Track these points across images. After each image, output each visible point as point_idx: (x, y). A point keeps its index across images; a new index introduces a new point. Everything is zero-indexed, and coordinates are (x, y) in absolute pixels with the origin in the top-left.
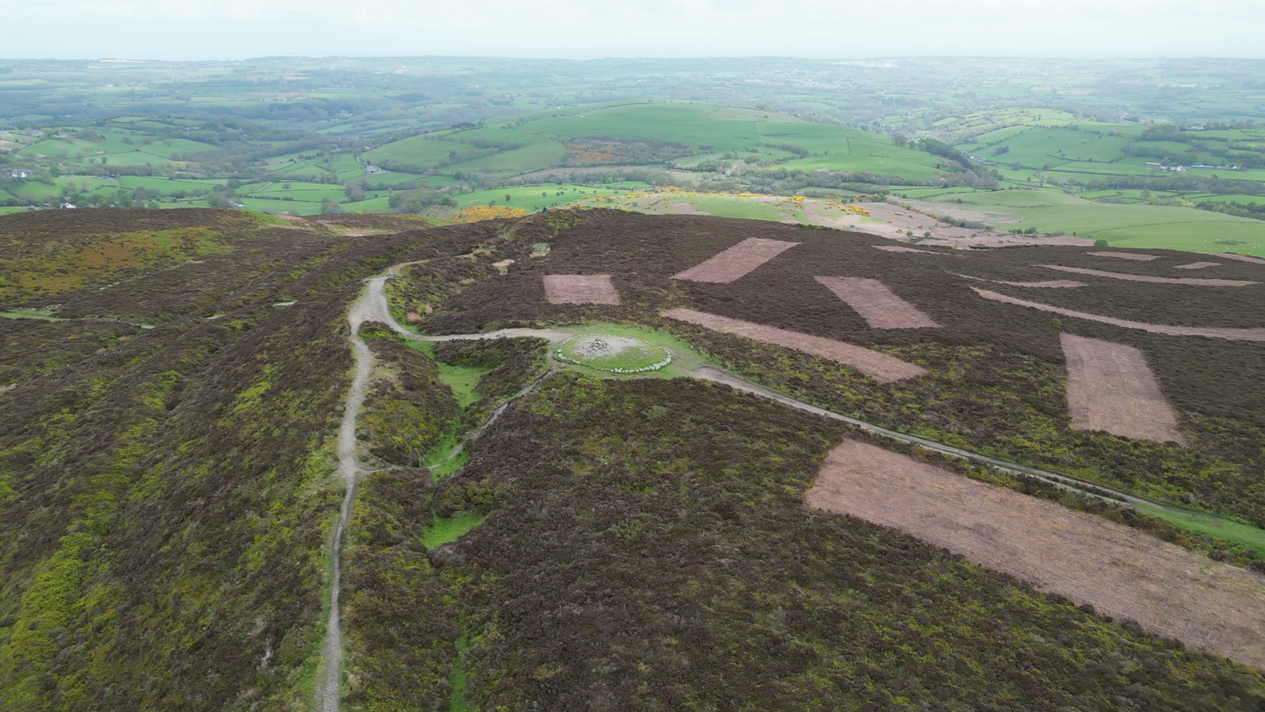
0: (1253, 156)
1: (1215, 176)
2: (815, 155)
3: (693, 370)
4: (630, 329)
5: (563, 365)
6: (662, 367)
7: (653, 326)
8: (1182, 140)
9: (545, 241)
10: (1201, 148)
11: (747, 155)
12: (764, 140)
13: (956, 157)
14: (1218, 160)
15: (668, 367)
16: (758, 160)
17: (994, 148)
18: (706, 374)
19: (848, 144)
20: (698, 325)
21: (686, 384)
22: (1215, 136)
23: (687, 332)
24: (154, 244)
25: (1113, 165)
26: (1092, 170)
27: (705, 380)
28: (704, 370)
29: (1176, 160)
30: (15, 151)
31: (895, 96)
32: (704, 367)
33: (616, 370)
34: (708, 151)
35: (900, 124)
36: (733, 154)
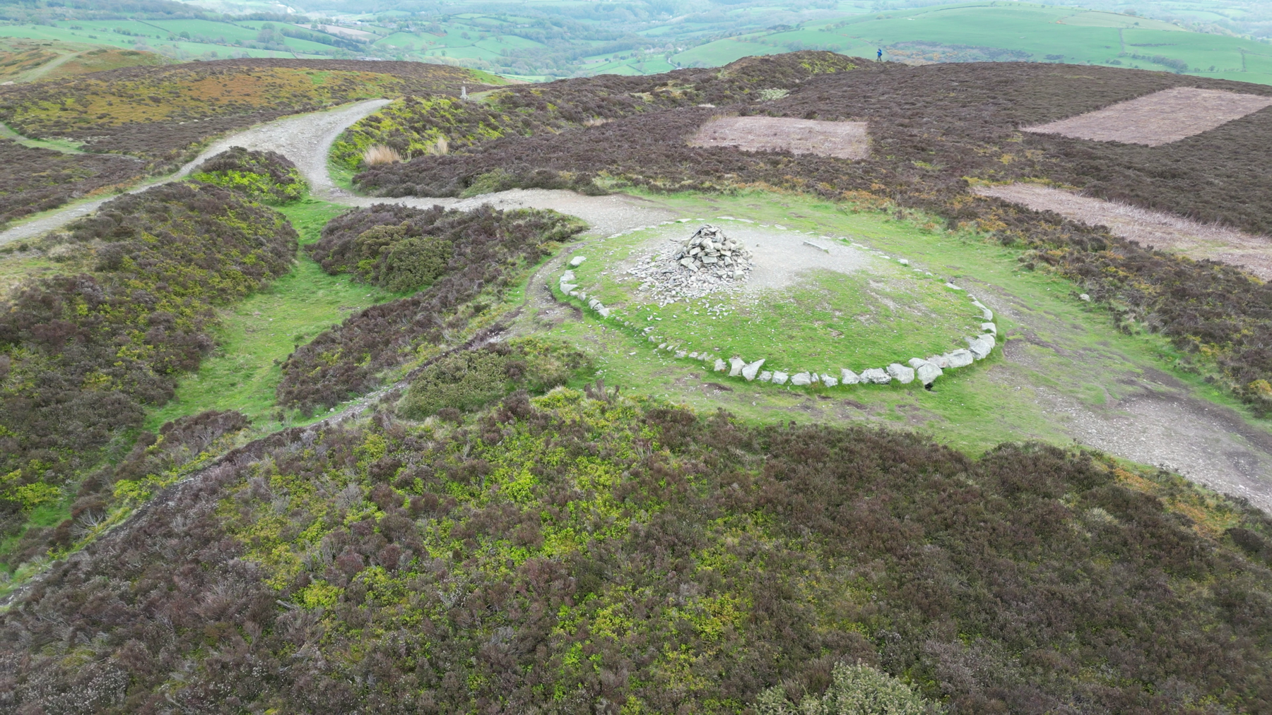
3: (1099, 408)
4: (864, 217)
5: (558, 312)
6: (949, 373)
7: (944, 213)
9: (785, 87)
15: (982, 375)
18: (1168, 435)
19: (1244, 58)
20: (1096, 228)
21: (1067, 500)
23: (1059, 244)
24: (301, 82)
27: (1172, 484)
28: (1153, 418)
30: (372, 42)
32: (1151, 395)
33: (737, 365)
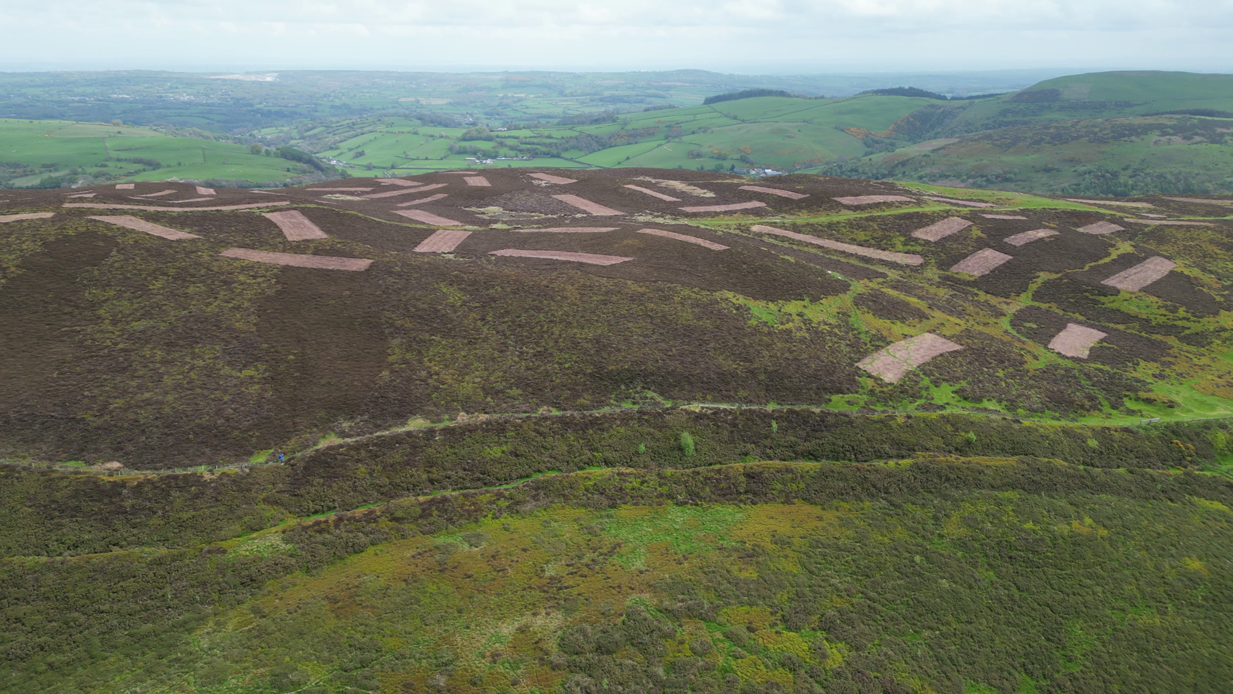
0: (535, 149)
1: (509, 165)
2: (169, 166)
8: (489, 139)
10: (502, 145)
11: (95, 170)
12: (113, 154)
13: (309, 161)
14: (512, 153)
16: (107, 174)
17: (352, 154)
19: (204, 154)
22: (512, 135)
25: (444, 161)
26: (428, 167)
29: (487, 155)
31: (273, 109)
34: (52, 169)
35: (276, 135)
36: (80, 170)
